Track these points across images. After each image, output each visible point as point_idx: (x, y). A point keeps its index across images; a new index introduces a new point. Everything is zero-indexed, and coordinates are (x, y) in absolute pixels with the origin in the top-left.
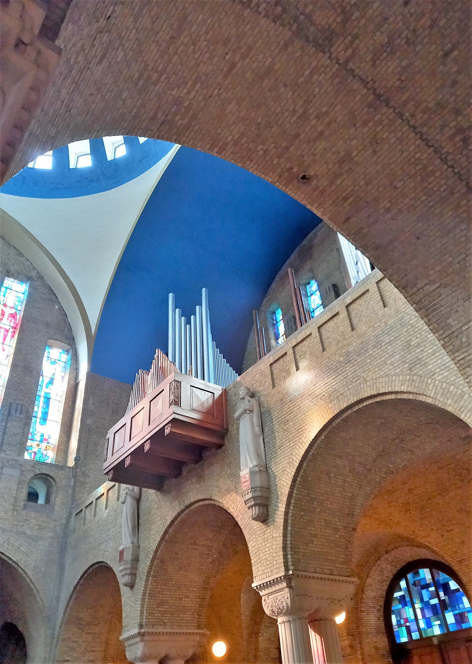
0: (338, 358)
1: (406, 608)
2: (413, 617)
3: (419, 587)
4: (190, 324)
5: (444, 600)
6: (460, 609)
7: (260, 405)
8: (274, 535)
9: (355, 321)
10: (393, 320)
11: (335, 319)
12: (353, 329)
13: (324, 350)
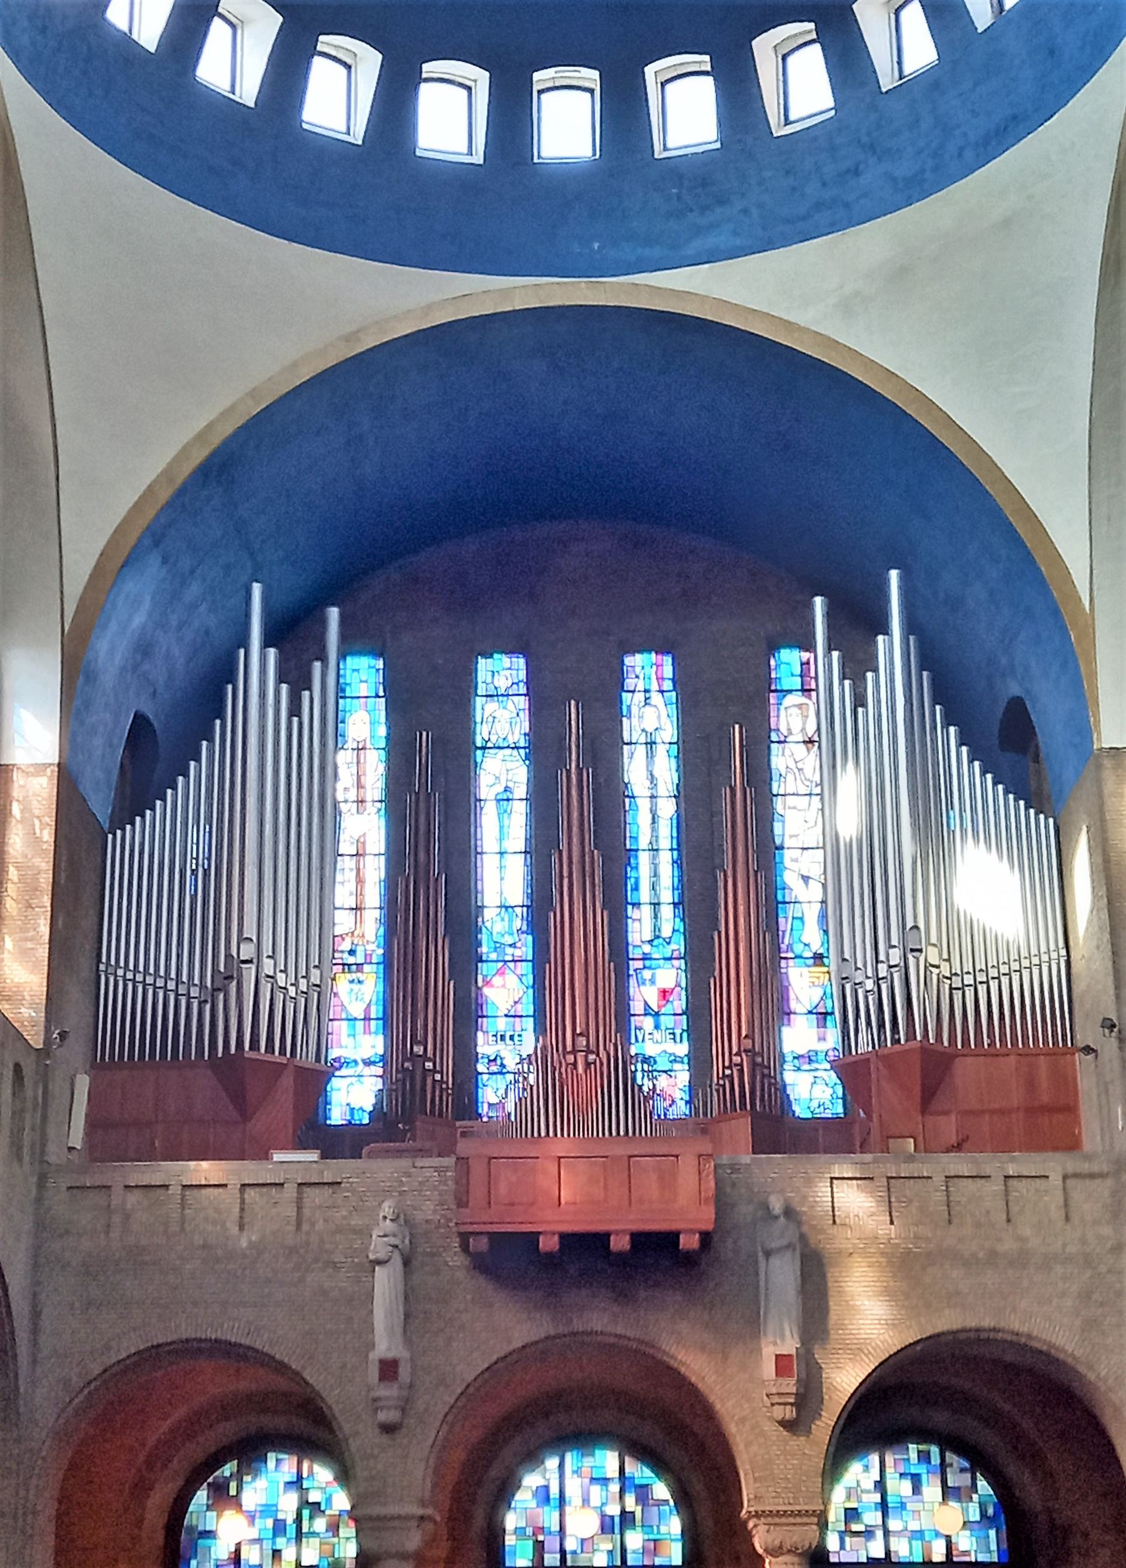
1: (547, 1509)
2: (555, 1527)
3: (587, 1481)
4: (299, 716)
5: (633, 1513)
6: (659, 1532)
7: (803, 1238)
8: (807, 1452)
9: (1015, 1209)
11: (980, 1182)
12: (1009, 1221)
13: (950, 1222)
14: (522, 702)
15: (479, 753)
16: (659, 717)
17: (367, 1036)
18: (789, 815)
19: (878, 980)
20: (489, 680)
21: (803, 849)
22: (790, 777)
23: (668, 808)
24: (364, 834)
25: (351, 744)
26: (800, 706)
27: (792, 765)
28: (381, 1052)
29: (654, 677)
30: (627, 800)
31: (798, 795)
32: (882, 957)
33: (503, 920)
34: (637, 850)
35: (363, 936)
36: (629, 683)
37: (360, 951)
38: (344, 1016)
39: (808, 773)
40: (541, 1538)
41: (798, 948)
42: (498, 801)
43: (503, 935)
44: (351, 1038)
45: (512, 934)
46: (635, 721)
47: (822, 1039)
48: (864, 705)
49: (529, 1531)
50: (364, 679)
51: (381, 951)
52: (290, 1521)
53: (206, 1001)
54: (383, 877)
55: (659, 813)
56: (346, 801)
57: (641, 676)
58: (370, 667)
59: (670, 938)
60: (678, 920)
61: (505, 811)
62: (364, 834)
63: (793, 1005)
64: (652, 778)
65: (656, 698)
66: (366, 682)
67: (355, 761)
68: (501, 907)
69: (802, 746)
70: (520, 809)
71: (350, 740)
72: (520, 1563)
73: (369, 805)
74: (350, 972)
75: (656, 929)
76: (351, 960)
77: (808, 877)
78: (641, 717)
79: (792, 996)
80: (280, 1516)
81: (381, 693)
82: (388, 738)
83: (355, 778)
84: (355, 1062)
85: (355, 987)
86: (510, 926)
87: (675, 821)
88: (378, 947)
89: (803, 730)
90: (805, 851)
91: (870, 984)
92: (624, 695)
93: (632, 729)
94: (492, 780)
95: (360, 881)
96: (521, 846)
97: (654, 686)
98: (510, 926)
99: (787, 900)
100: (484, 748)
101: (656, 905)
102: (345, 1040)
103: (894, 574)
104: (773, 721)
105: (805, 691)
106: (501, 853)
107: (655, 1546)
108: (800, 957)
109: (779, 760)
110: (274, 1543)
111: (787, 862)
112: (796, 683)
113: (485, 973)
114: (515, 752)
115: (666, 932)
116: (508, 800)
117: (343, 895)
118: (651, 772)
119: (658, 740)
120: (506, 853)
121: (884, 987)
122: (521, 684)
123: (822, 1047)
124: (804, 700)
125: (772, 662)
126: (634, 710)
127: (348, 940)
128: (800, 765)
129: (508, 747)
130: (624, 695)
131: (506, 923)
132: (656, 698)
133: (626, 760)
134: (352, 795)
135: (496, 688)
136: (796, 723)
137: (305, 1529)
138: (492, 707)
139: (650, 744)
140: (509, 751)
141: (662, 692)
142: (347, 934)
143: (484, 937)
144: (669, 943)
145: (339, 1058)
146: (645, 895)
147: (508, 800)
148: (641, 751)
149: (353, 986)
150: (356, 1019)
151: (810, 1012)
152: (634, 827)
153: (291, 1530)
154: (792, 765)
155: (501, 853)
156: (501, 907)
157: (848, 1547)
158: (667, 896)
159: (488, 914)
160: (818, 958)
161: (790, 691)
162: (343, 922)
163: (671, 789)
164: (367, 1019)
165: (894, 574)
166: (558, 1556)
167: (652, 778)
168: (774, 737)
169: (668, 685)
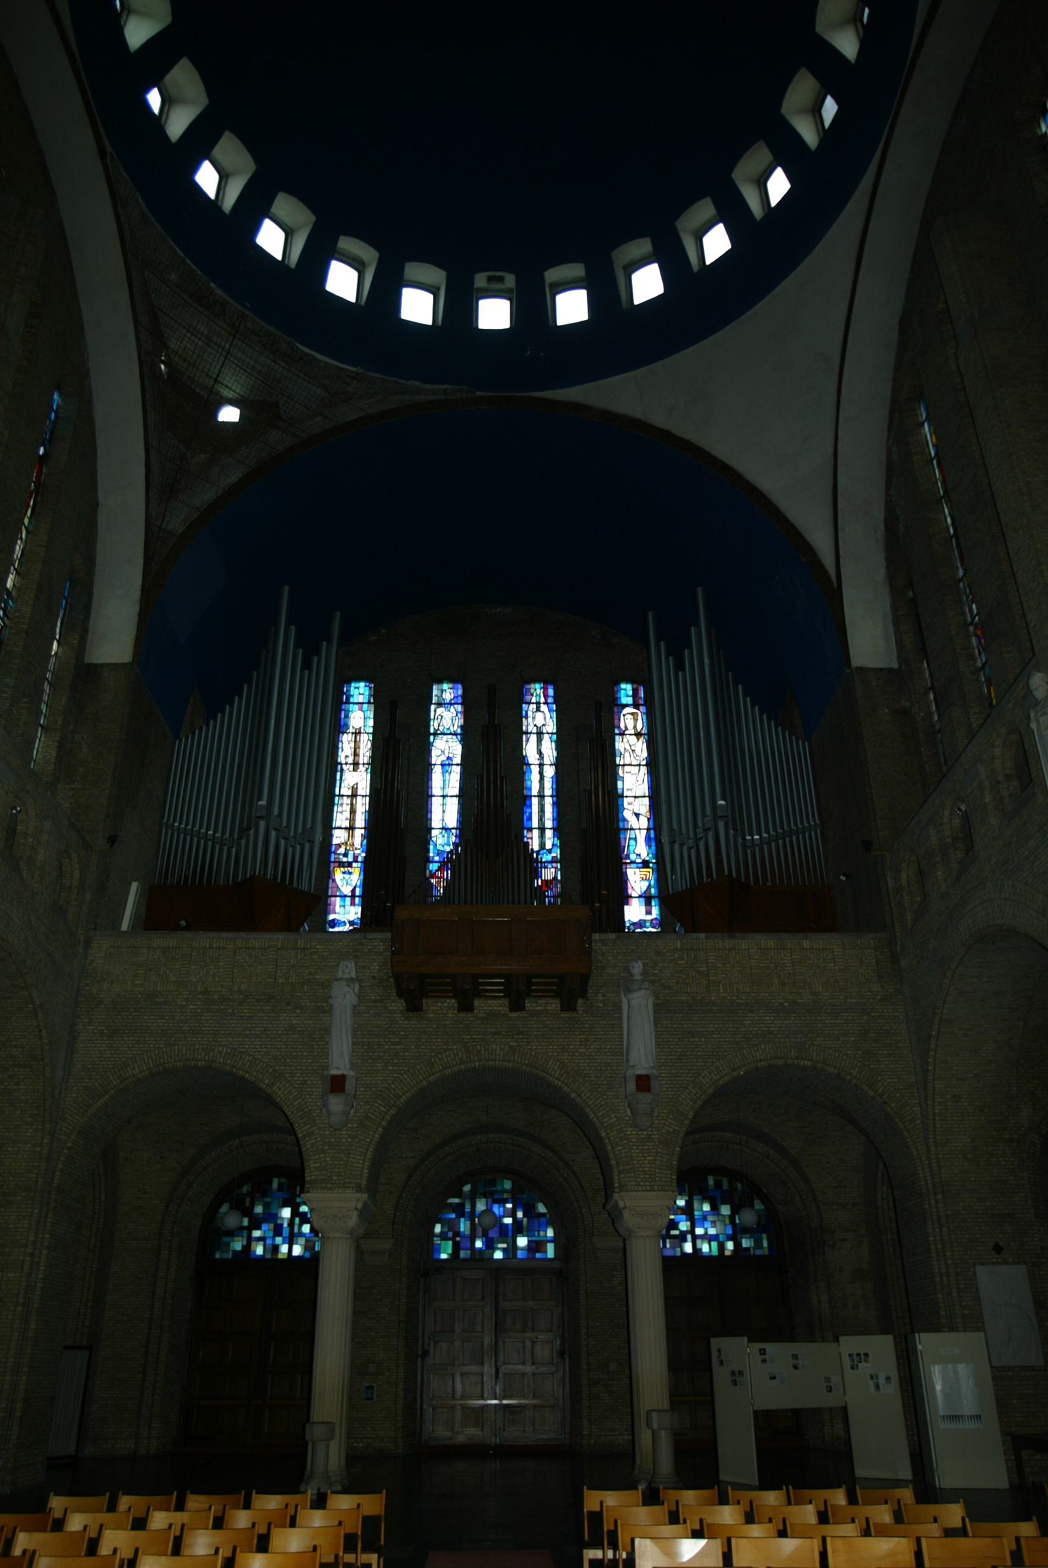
0: (782, 1001)
1: (462, 1220)
6: (539, 1235)
10: (854, 1001)
14: (459, 708)
15: (432, 738)
16: (545, 718)
17: (352, 907)
18: (627, 777)
19: (697, 840)
20: (439, 695)
21: (635, 797)
22: (627, 755)
23: (549, 772)
24: (357, 784)
25: (351, 730)
26: (632, 714)
27: (628, 747)
28: (360, 916)
29: (542, 695)
30: (525, 767)
31: (631, 765)
32: (700, 824)
33: (443, 836)
34: (531, 796)
35: (353, 844)
36: (528, 698)
37: (351, 854)
38: (338, 894)
39: (638, 752)
40: (458, 1239)
41: (633, 857)
42: (443, 765)
43: (443, 846)
44: (342, 908)
45: (449, 845)
46: (530, 720)
47: (649, 912)
48: (683, 669)
49: (450, 1234)
50: (361, 692)
51: (364, 855)
52: (285, 1225)
53: (232, 847)
54: (367, 809)
55: (545, 774)
56: (346, 764)
57: (535, 695)
58: (365, 686)
59: (551, 849)
60: (556, 839)
61: (447, 771)
62: (357, 784)
63: (630, 891)
64: (540, 753)
65: (544, 708)
66: (363, 694)
67: (353, 739)
68: (443, 828)
69: (634, 737)
70: (456, 770)
71: (351, 728)
72: (444, 1256)
73: (361, 766)
74: (344, 867)
75: (542, 845)
76: (345, 859)
77: (639, 814)
78: (534, 718)
79: (629, 886)
80: (279, 1222)
81: (372, 701)
82: (374, 727)
83: (353, 750)
84: (344, 922)
85: (347, 876)
86: (448, 841)
87: (554, 779)
88: (363, 852)
89: (635, 727)
90: (637, 799)
91: (691, 843)
92: (524, 705)
93: (529, 725)
94: (440, 752)
95: (353, 811)
96: (456, 792)
97: (542, 700)
98: (448, 841)
99: (626, 827)
100: (435, 734)
101: (542, 829)
102: (337, 909)
103: (700, 590)
104: (616, 721)
105: (636, 705)
106: (444, 796)
107: (536, 1246)
108: (634, 862)
109: (620, 745)
110: (274, 1240)
111: (626, 805)
112: (630, 700)
113: (431, 869)
114: (454, 737)
115: (548, 845)
116: (449, 765)
117: (341, 818)
118: (540, 750)
119: (544, 731)
120: (447, 796)
121: (702, 844)
122: (459, 698)
123: (649, 917)
124: (635, 711)
125: (616, 689)
126: (530, 714)
127: (343, 847)
128: (633, 748)
129: (450, 734)
130: (524, 705)
131: (446, 839)
132: (544, 708)
133: (524, 743)
134: (350, 760)
135: (444, 700)
136: (630, 724)
137: (296, 1230)
138: (440, 710)
139: (540, 734)
140: (451, 736)
141: (546, 703)
142: (343, 844)
143: (431, 847)
144: (550, 853)
145: (334, 920)
146: (535, 823)
147: (449, 765)
148: (533, 738)
149: (345, 875)
150: (346, 896)
151: (640, 896)
152: (529, 783)
153: (286, 1232)
154: (628, 747)
155: (444, 796)
156: (443, 828)
157: (668, 1246)
158: (549, 824)
159: (434, 833)
160: (645, 864)
161: (627, 706)
162: (339, 837)
163: (552, 760)
164: (353, 896)
165: (700, 590)
166: (469, 1252)
167: (540, 753)
168: (617, 731)
169: (550, 700)
